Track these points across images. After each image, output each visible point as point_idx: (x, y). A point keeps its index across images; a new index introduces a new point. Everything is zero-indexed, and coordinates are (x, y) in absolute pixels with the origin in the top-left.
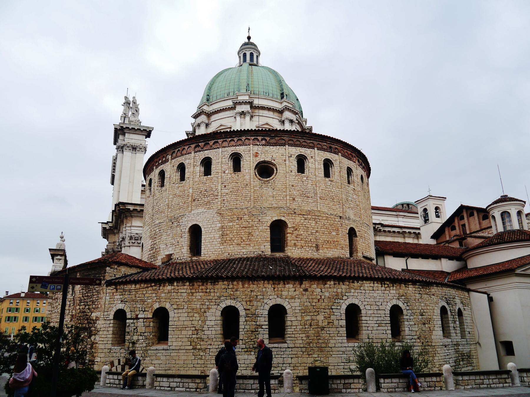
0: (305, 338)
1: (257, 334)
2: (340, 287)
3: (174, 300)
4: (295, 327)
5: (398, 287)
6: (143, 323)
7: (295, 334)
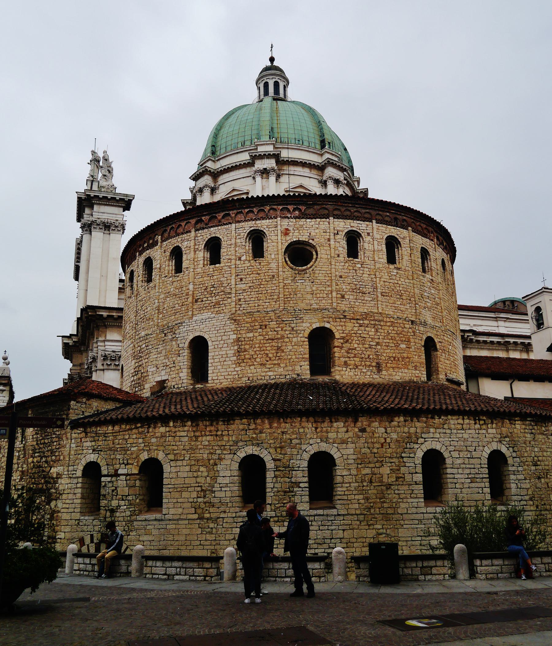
0: (362, 501)
1: (292, 495)
2: (413, 424)
3: (171, 447)
4: (347, 485)
5: (500, 424)
6: (125, 482)
7: (347, 495)
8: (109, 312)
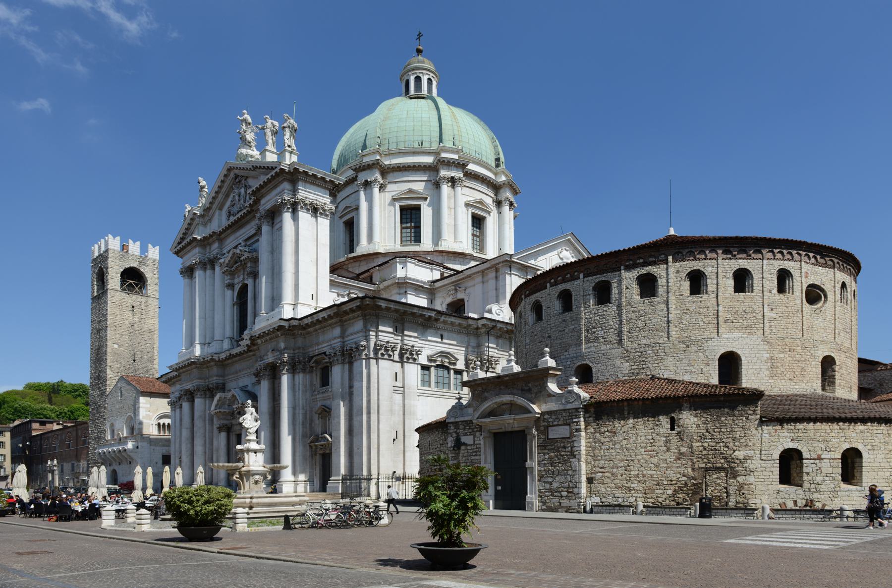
3: (869, 441)
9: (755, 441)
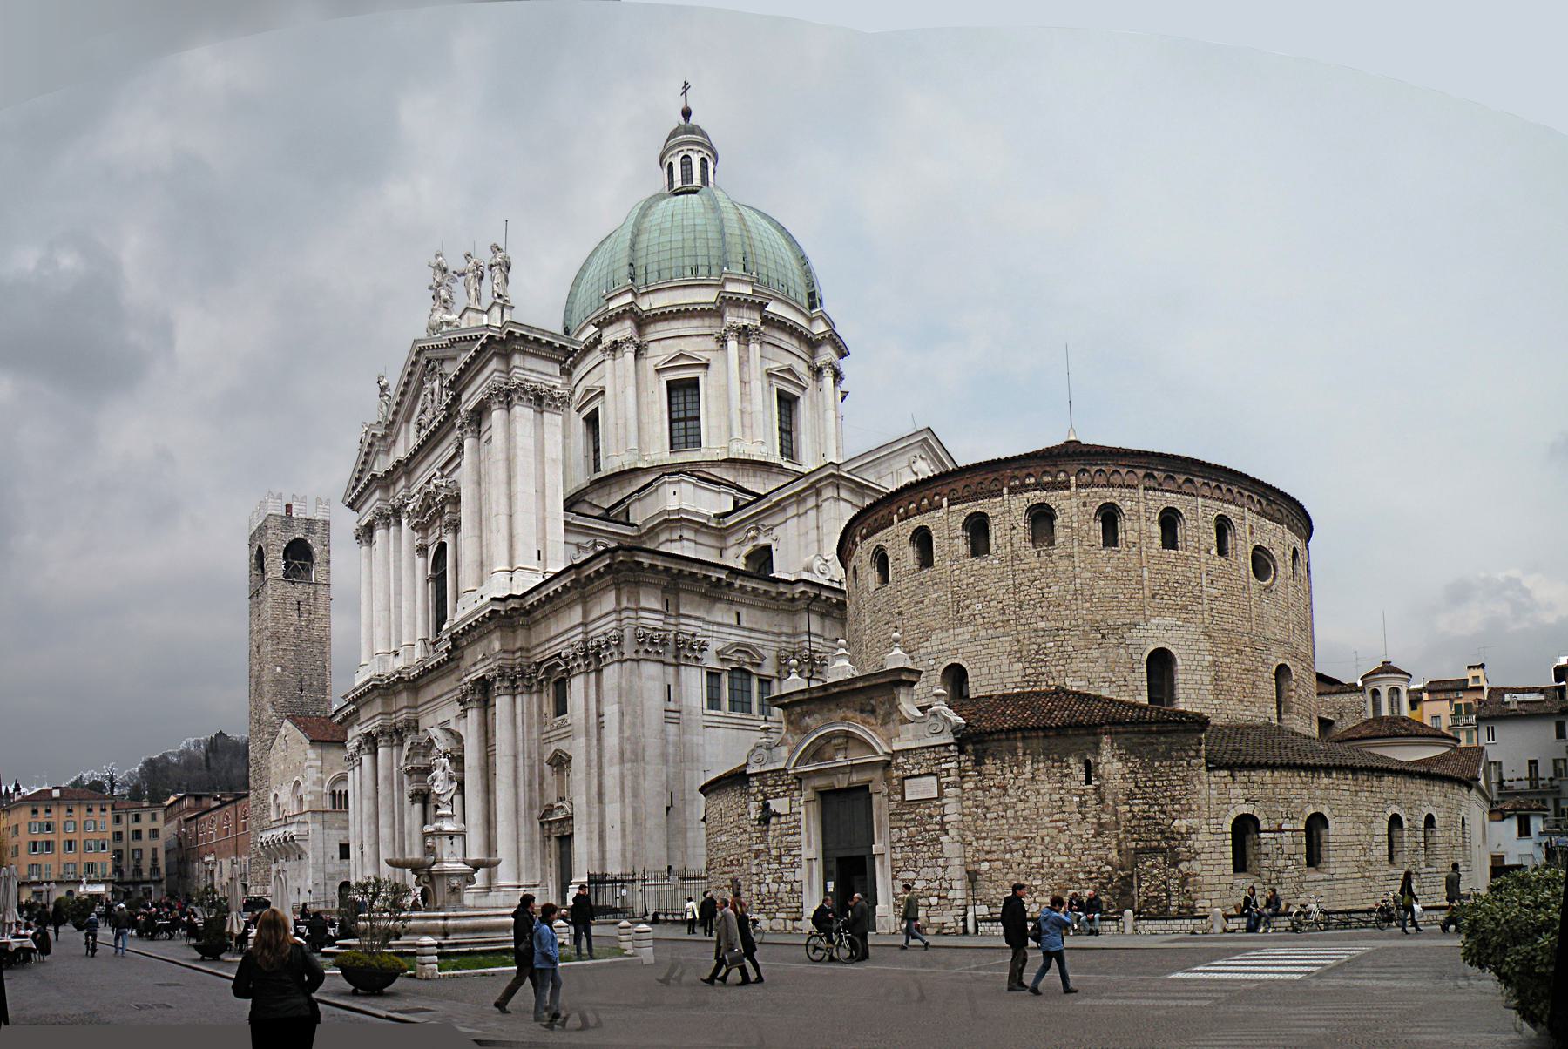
8: (652, 559)
9: (1200, 802)
